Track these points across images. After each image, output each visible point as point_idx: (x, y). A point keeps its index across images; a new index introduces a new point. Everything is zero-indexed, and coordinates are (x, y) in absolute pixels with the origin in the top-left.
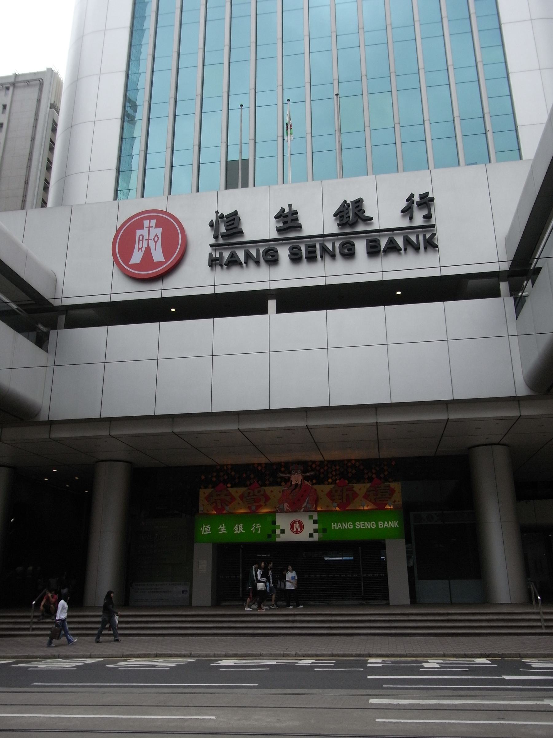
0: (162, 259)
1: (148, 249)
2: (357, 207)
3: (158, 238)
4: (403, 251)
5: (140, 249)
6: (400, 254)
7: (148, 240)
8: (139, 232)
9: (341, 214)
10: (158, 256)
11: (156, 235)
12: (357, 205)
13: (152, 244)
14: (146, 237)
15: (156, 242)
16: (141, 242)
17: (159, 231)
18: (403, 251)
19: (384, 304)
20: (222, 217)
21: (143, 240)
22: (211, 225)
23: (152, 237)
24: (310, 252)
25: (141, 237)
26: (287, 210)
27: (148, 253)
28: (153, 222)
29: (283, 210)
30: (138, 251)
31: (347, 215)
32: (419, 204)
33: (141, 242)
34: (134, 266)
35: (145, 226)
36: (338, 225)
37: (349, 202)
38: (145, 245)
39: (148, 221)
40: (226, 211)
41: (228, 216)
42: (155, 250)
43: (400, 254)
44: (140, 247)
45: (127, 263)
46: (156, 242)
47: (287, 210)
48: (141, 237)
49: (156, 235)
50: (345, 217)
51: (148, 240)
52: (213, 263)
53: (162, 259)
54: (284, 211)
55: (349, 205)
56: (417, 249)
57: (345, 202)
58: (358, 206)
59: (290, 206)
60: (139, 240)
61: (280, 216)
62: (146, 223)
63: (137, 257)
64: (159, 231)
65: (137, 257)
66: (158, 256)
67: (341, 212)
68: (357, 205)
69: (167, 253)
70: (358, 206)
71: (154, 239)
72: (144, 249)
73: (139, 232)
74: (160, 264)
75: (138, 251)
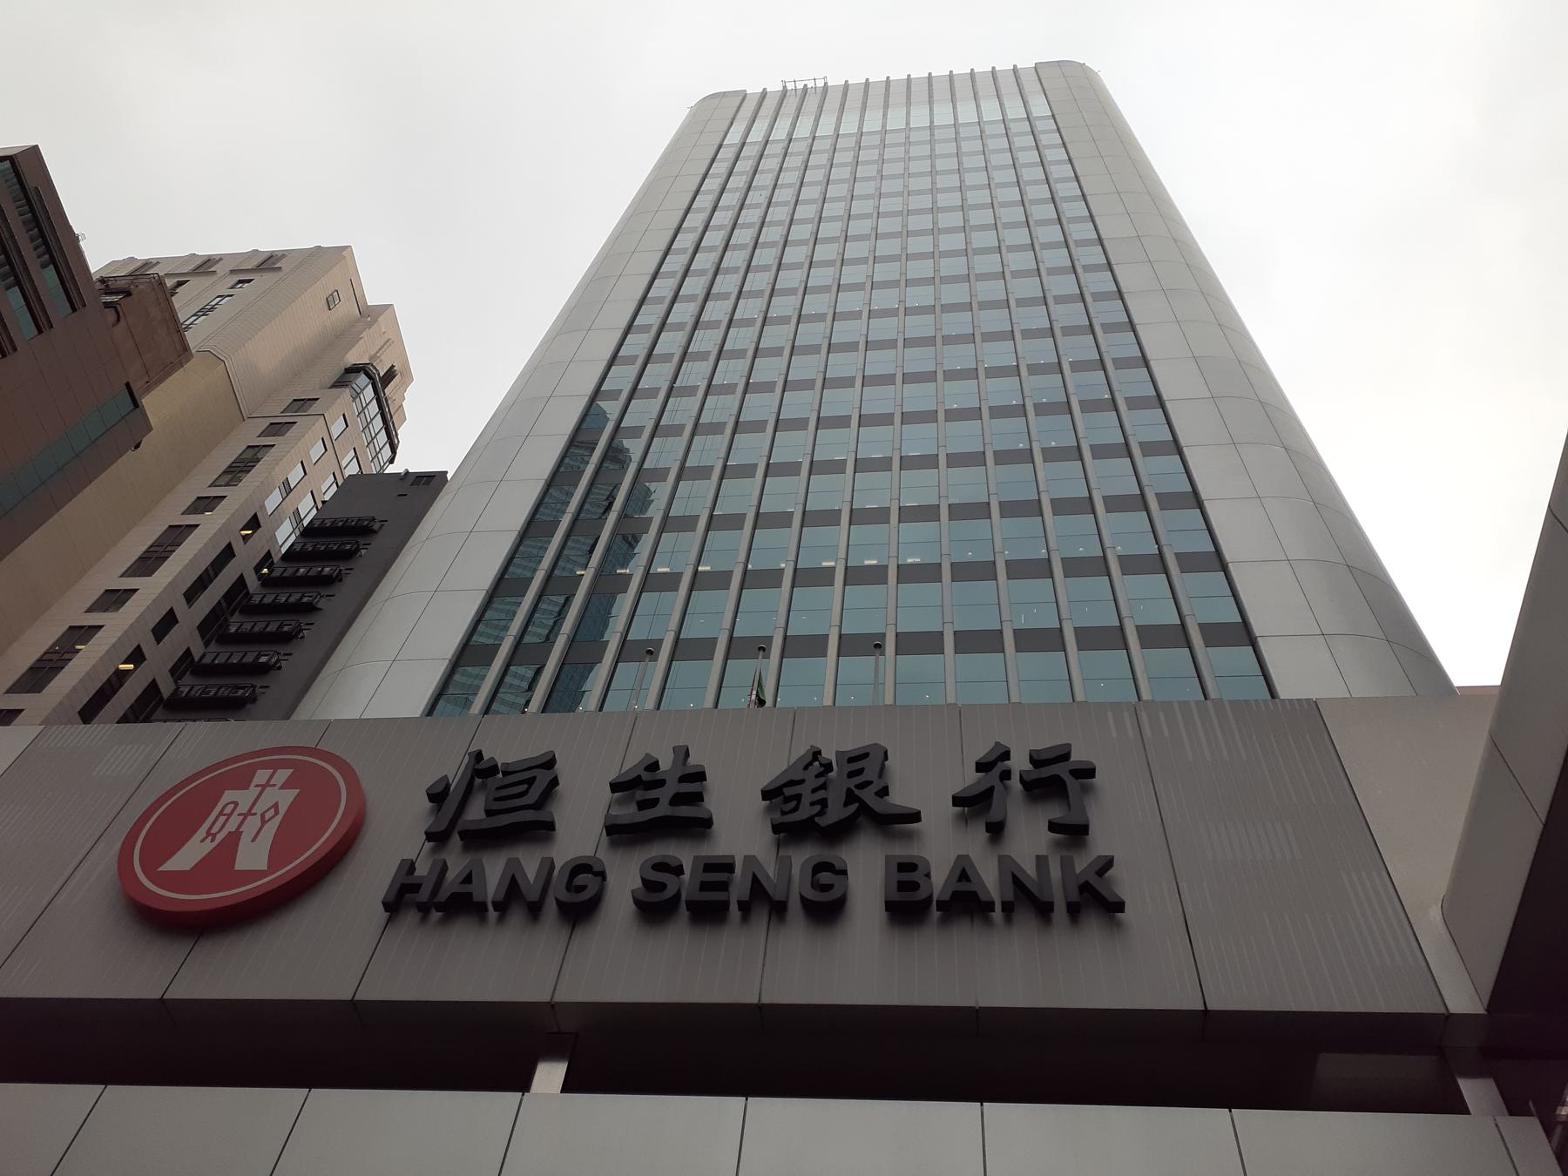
2: (851, 775)
4: (997, 915)
6: (988, 921)
14: (243, 808)
16: (223, 819)
18: (997, 915)
19: (981, 1097)
25: (228, 810)
31: (821, 794)
32: (1029, 785)
33: (223, 819)
36: (776, 829)
37: (829, 754)
43: (988, 921)
50: (806, 801)
55: (828, 767)
56: (1044, 910)
57: (816, 754)
58: (860, 771)
60: (221, 813)
70: (851, 775)
71: (263, 816)
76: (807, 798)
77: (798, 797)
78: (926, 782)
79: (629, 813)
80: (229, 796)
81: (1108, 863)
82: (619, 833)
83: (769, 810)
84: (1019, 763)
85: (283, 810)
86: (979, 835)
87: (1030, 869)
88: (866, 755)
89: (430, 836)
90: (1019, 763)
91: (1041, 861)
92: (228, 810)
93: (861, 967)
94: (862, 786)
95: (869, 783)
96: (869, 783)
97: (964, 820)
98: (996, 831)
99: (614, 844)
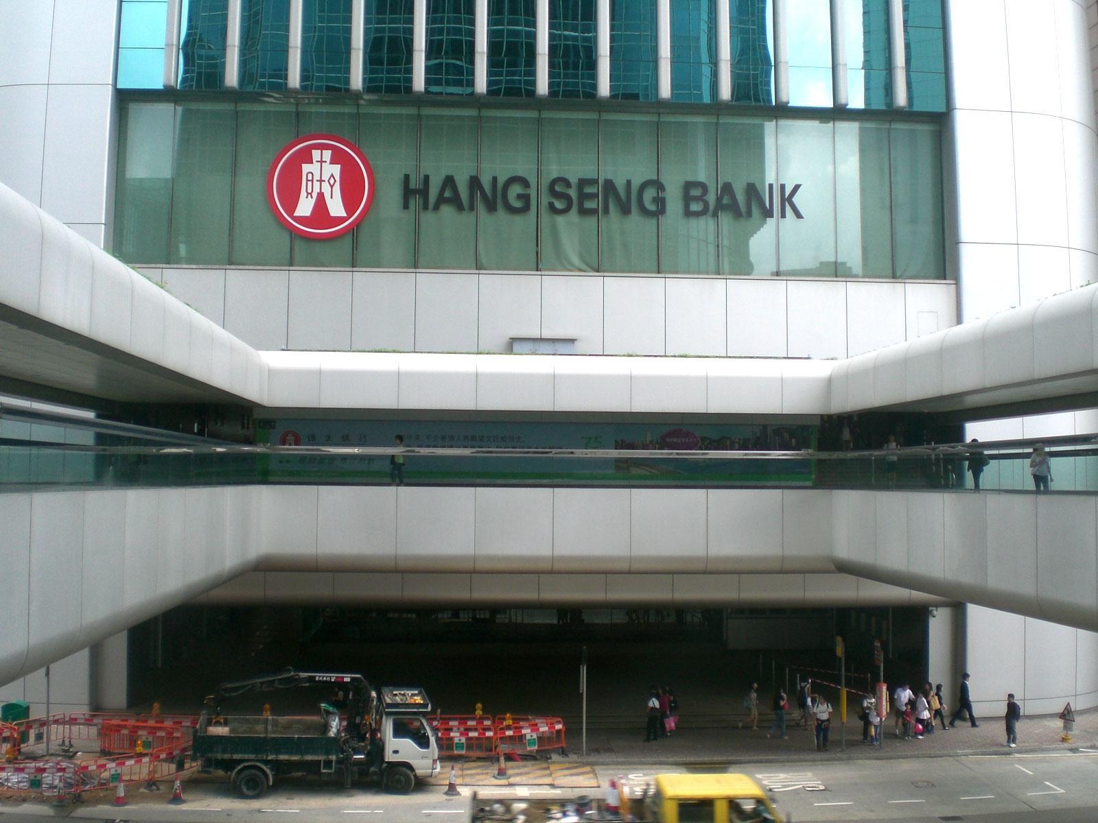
0: (344, 214)
1: (321, 196)
3: (335, 181)
5: (309, 194)
7: (321, 181)
8: (306, 168)
10: (336, 208)
11: (332, 176)
13: (326, 189)
14: (317, 177)
15: (332, 187)
16: (310, 183)
17: (336, 169)
21: (312, 181)
23: (326, 177)
25: (310, 178)
27: (321, 202)
28: (327, 154)
30: (307, 197)
33: (310, 183)
34: (300, 220)
35: (314, 160)
38: (316, 190)
39: (320, 151)
42: (332, 198)
44: (309, 191)
45: (291, 213)
46: (332, 187)
48: (310, 175)
49: (332, 176)
53: (344, 214)
60: (307, 180)
62: (316, 154)
63: (305, 207)
64: (336, 169)
65: (305, 207)
66: (336, 208)
72: (315, 195)
73: (306, 168)
74: (340, 220)
75: (307, 197)
85: (337, 177)
92: (310, 178)
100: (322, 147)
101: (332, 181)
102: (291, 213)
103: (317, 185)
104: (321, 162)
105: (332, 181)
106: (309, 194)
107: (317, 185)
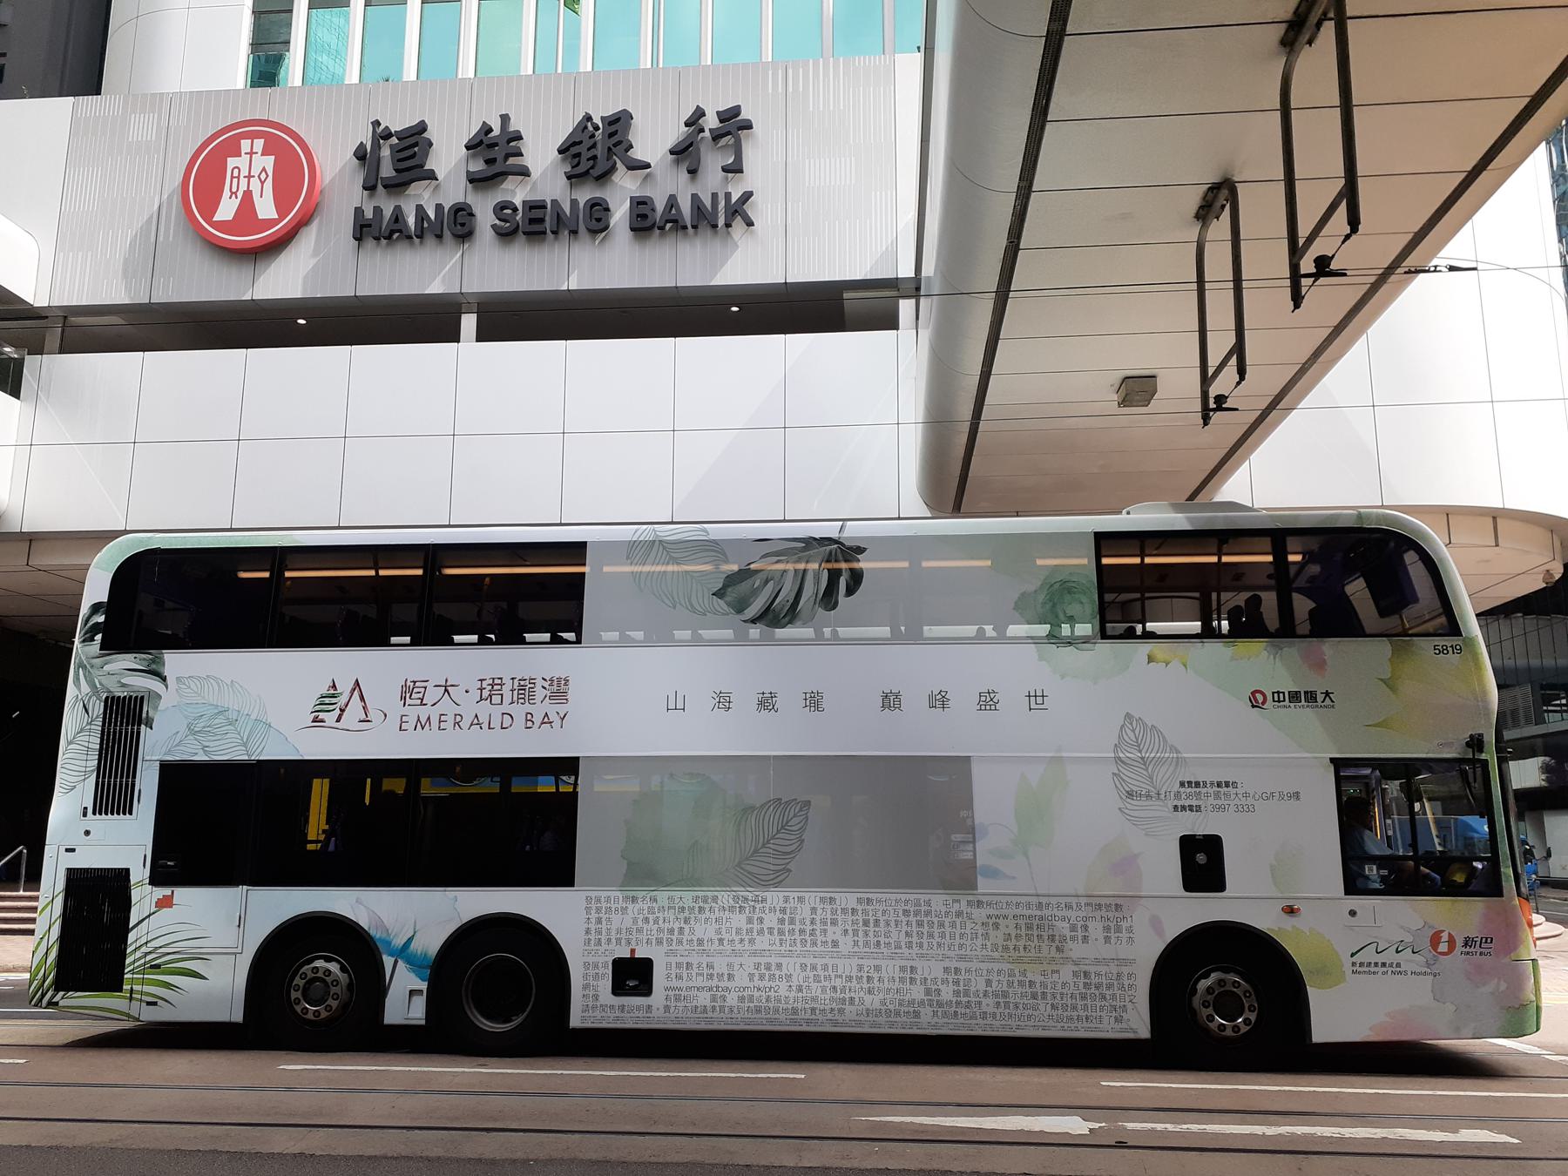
1: (248, 194)
2: (611, 135)
5: (233, 194)
7: (249, 177)
9: (574, 150)
10: (266, 208)
12: (613, 128)
13: (255, 186)
20: (387, 135)
22: (360, 154)
23: (255, 172)
24: (532, 221)
25: (236, 173)
26: (496, 131)
29: (487, 130)
31: (590, 154)
34: (220, 226)
38: (243, 187)
40: (398, 122)
41: (402, 135)
47: (496, 131)
51: (249, 177)
52: (364, 230)
54: (491, 130)
55: (597, 128)
57: (588, 118)
58: (615, 133)
59: (505, 119)
61: (481, 144)
63: (227, 209)
65: (227, 209)
66: (266, 208)
67: (575, 144)
68: (613, 128)
69: (282, 205)
70: (615, 133)
72: (240, 194)
76: (586, 155)
77: (578, 155)
78: (653, 140)
79: (478, 166)
80: (232, 162)
81: (747, 196)
82: (475, 180)
83: (564, 160)
84: (711, 122)
86: (684, 176)
87: (708, 203)
88: (618, 120)
89: (365, 188)
90: (711, 122)
91: (714, 196)
92: (236, 173)
93: (613, 265)
94: (615, 145)
95: (620, 143)
96: (620, 143)
97: (677, 162)
98: (693, 172)
99: (476, 189)
100: (252, 136)
101: (263, 176)
102: (208, 217)
103: (244, 182)
104: (251, 153)
105: (263, 176)
106: (233, 194)
107: (244, 182)
